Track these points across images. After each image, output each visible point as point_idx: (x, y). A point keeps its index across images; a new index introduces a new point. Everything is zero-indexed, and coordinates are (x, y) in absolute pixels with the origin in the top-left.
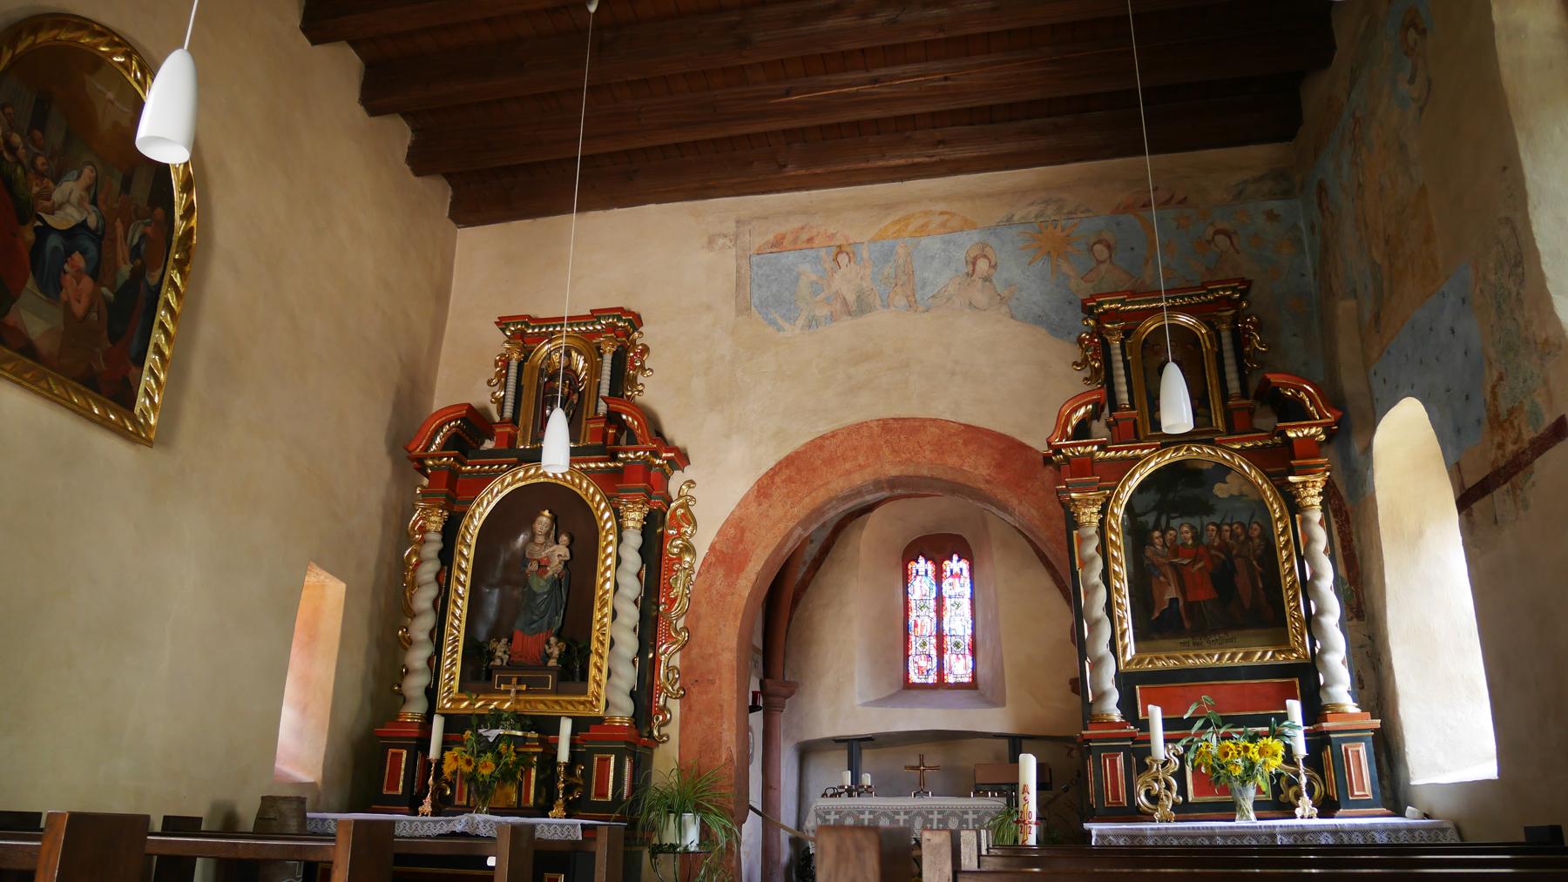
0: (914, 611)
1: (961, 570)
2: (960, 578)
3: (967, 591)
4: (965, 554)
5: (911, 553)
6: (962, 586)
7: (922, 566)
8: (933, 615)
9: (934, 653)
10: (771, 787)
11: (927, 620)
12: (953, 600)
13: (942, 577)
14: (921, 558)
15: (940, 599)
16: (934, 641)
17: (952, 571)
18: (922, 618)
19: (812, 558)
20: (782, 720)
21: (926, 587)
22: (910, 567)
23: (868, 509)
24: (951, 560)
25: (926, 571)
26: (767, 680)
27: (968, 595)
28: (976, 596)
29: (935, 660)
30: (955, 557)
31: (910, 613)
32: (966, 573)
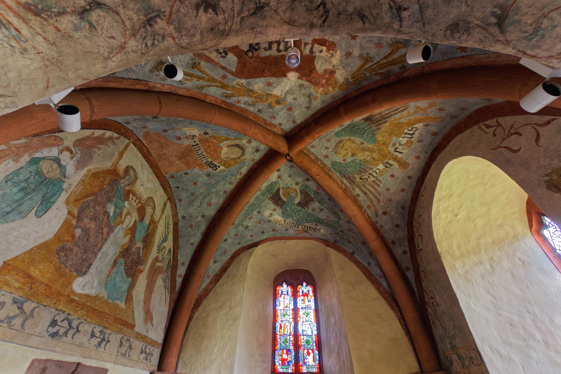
0: (280, 317)
4: (312, 282)
5: (278, 281)
6: (309, 301)
7: (285, 288)
8: (291, 320)
13: (297, 296)
15: (296, 311)
17: (303, 292)
18: (284, 322)
19: (215, 273)
21: (287, 301)
22: (278, 289)
23: (256, 245)
24: (302, 285)
25: (288, 292)
27: (313, 308)
28: (320, 307)
30: (305, 284)
31: (277, 319)
32: (311, 293)
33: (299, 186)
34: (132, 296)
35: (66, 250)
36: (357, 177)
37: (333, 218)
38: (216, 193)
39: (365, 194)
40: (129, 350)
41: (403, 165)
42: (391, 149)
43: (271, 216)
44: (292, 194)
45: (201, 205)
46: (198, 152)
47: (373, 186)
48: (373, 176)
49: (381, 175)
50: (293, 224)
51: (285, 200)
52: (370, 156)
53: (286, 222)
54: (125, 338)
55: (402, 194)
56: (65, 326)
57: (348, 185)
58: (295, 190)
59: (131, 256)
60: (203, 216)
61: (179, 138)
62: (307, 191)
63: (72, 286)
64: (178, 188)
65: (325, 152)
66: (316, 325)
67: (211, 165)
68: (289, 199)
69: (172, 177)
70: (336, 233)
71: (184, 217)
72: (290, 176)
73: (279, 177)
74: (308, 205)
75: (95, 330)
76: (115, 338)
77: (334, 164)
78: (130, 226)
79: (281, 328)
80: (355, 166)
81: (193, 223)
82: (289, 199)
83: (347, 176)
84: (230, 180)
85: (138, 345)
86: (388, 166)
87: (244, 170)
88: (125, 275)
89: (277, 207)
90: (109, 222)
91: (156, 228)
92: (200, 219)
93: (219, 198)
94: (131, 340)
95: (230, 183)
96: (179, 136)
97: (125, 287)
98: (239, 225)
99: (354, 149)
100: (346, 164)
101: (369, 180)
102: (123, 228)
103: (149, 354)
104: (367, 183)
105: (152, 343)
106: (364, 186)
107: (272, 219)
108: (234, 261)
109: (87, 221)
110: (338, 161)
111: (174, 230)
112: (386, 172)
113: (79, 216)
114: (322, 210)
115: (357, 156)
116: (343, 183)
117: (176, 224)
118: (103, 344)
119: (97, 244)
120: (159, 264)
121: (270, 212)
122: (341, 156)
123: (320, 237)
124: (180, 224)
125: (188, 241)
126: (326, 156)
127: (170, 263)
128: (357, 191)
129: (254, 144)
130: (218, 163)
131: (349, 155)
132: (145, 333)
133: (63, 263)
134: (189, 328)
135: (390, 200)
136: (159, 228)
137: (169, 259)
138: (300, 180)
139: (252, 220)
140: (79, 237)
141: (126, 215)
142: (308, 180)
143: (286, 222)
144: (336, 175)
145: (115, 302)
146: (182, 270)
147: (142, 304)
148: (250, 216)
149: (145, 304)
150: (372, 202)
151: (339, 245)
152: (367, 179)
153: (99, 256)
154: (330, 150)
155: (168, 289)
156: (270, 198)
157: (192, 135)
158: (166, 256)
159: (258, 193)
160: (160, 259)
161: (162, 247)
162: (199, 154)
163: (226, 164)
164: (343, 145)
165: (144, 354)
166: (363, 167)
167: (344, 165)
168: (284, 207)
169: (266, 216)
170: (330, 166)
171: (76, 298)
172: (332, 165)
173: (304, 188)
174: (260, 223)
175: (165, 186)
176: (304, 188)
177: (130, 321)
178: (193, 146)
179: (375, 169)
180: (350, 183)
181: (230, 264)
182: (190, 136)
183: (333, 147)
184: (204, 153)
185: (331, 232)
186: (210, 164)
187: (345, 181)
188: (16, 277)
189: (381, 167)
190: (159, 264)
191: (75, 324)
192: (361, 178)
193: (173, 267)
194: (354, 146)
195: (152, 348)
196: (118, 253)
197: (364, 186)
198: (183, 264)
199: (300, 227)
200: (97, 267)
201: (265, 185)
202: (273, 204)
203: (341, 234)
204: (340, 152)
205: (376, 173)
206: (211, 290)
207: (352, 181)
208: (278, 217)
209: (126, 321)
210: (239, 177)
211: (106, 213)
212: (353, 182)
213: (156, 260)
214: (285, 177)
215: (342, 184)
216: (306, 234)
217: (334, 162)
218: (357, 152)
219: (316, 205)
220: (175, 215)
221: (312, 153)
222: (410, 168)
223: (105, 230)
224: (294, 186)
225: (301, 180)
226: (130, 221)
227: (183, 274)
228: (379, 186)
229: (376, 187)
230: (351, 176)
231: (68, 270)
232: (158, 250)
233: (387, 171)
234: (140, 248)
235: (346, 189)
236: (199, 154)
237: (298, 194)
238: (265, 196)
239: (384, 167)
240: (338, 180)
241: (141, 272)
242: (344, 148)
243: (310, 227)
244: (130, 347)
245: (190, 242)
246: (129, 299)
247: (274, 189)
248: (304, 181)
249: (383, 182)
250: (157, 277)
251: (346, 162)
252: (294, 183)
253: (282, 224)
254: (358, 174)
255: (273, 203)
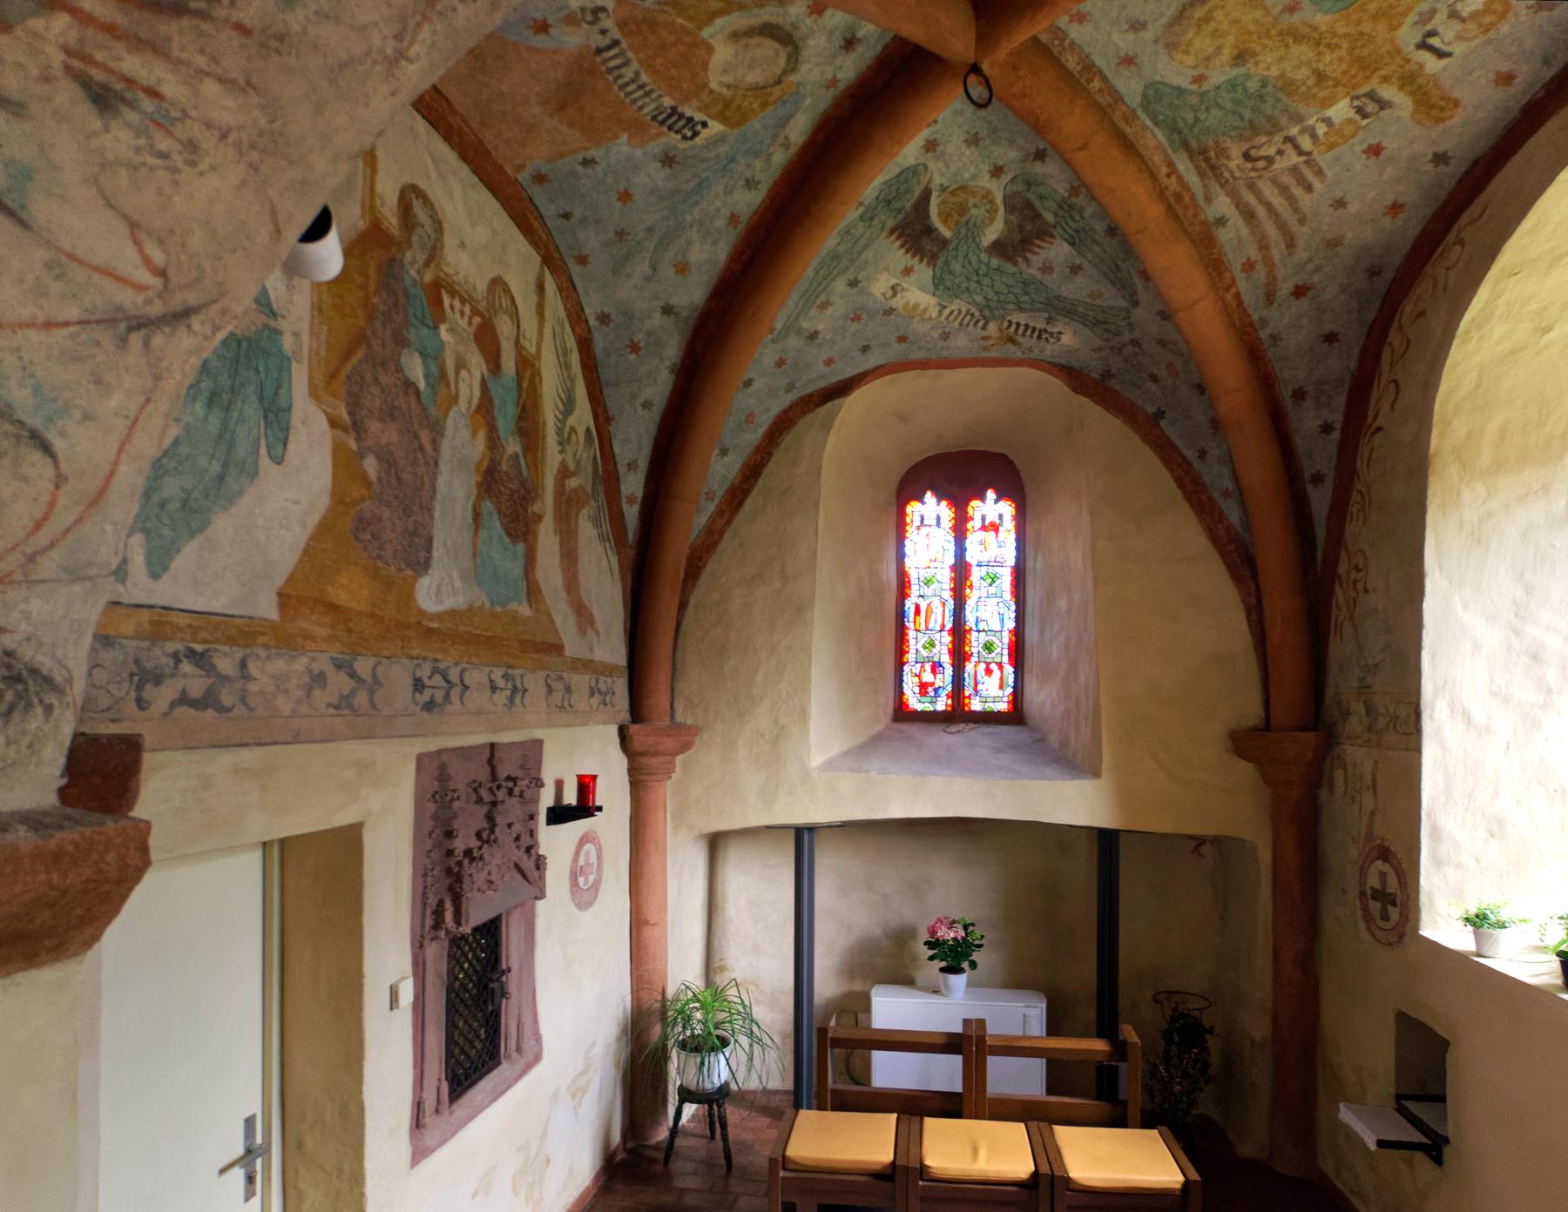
1: (1001, 517)
2: (997, 531)
3: (1010, 555)
4: (1012, 488)
5: (910, 487)
8: (947, 595)
9: (946, 659)
10: (647, 923)
11: (936, 603)
12: (984, 569)
14: (929, 494)
15: (961, 572)
16: (947, 638)
19: (727, 485)
20: (668, 793)
22: (909, 509)
23: (842, 389)
24: (982, 498)
25: (938, 519)
26: (634, 729)
29: (949, 671)
33: (1006, 178)
34: (537, 582)
35: (369, 525)
36: (1235, 151)
37: (1111, 298)
38: (701, 225)
39: (1249, 216)
40: (568, 696)
41: (1432, 107)
42: (1408, 35)
43: (895, 295)
44: (974, 212)
45: (655, 270)
46: (619, 77)
47: (1284, 190)
48: (1296, 147)
49: (1331, 147)
50: (968, 318)
51: (947, 234)
52: (1309, 63)
53: (947, 312)
54: (553, 675)
55: (1387, 221)
56: (439, 685)
57: (1192, 178)
58: (988, 197)
59: (506, 487)
60: (667, 310)
61: (542, 27)
62: (1032, 197)
63: (415, 600)
64: (567, 216)
65: (1124, 42)
66: (1013, 607)
67: (673, 120)
68: (963, 232)
69: (540, 178)
70: (1112, 348)
71: (604, 319)
72: (973, 141)
73: (930, 146)
74: (1030, 251)
75: (493, 677)
76: (534, 682)
77: (1155, 94)
78: (475, 401)
79: (917, 612)
80: (1236, 102)
81: (639, 337)
82: (963, 232)
83: (1194, 143)
84: (748, 174)
85: (581, 681)
86: (1371, 107)
87: (799, 129)
88: (507, 540)
89: (916, 259)
90: (425, 409)
91: (537, 379)
92: (657, 320)
93: (715, 243)
94: (565, 675)
95: (750, 184)
96: (538, 16)
97: (516, 568)
98: (786, 331)
99: (1251, 33)
100: (1203, 95)
101: (1280, 164)
102: (463, 415)
103: (606, 694)
104: (1267, 174)
105: (607, 670)
106: (1251, 186)
107: (897, 303)
108: (778, 444)
109: (374, 426)
110: (1175, 80)
111: (584, 366)
112: (1353, 136)
113: (354, 423)
114: (1075, 269)
115: (1257, 64)
116: (1173, 171)
117: (585, 344)
118: (518, 700)
119: (423, 484)
120: (572, 483)
121: (893, 281)
122: (1191, 61)
123: (1056, 361)
124: (599, 342)
125: (634, 397)
126: (1128, 61)
127: (597, 469)
128: (1222, 205)
129: (835, 18)
130: (699, 109)
131: (1227, 53)
132: (586, 655)
133: (379, 557)
134: (683, 627)
135: (1334, 243)
136: (544, 373)
137: (591, 459)
138: (1009, 155)
139: (830, 311)
140: (379, 478)
141: (457, 373)
142: (1040, 156)
143: (947, 312)
144: (1154, 139)
145: (508, 607)
146: (633, 485)
147: (563, 594)
148: (823, 298)
149: (568, 593)
150: (1264, 247)
151: (1117, 387)
152: (1270, 161)
153: (437, 514)
154: (1148, 35)
155: (609, 541)
156: (892, 231)
157: (590, 5)
158: (584, 454)
159: (852, 215)
160: (572, 466)
161: (567, 430)
162: (627, 84)
163: (731, 111)
164: (1210, 11)
165: (596, 695)
166: (1268, 108)
167: (1194, 100)
168: (940, 262)
169: (879, 296)
170: (1134, 101)
171: (435, 625)
172: (1144, 96)
173: (1020, 187)
174: (856, 318)
175: (524, 216)
176: (1020, 187)
177: (550, 639)
178: (599, 51)
179: (1311, 122)
180: (1202, 175)
181: (770, 455)
182: (583, 10)
183: (1164, 20)
184: (644, 78)
185: (1098, 343)
186: (670, 116)
187: (1183, 164)
188: (314, 618)
189: (1341, 110)
190: (572, 483)
191: (454, 675)
192: (1247, 156)
193: (609, 477)
194: (1255, 22)
195: (609, 680)
196: (475, 491)
197: (1251, 186)
198: (632, 466)
199: (992, 328)
200: (445, 542)
201: (879, 180)
202: (903, 251)
203: (1129, 349)
204: (1190, 43)
205: (1314, 136)
206: (722, 532)
207: (1210, 166)
208: (918, 295)
209: (543, 643)
210: (780, 158)
211: (409, 385)
212: (1213, 168)
213: (564, 473)
214: (954, 143)
215: (1169, 175)
216: (1011, 348)
217: (1154, 83)
218: (1258, 49)
219: (1057, 252)
220: (576, 314)
221: (1073, 43)
222: (1455, 120)
223: (425, 436)
224: (986, 182)
225: (1013, 154)
226: (471, 387)
227: (639, 494)
228: (1309, 188)
229: (1297, 191)
230: (1210, 143)
231: (393, 569)
232: (560, 443)
233: (1359, 128)
234: (517, 456)
235: (1178, 197)
236: (627, 84)
237: (996, 211)
238: (876, 222)
239: (1352, 114)
240: (1157, 158)
241: (539, 518)
242: (1209, 28)
243: (1027, 326)
244: (568, 690)
245: (641, 400)
246: (533, 592)
247: (908, 196)
248: (1024, 159)
249: (1329, 173)
250: (577, 515)
251: (1206, 87)
252: (986, 167)
253: (930, 318)
254: (1241, 137)
255: (902, 246)
